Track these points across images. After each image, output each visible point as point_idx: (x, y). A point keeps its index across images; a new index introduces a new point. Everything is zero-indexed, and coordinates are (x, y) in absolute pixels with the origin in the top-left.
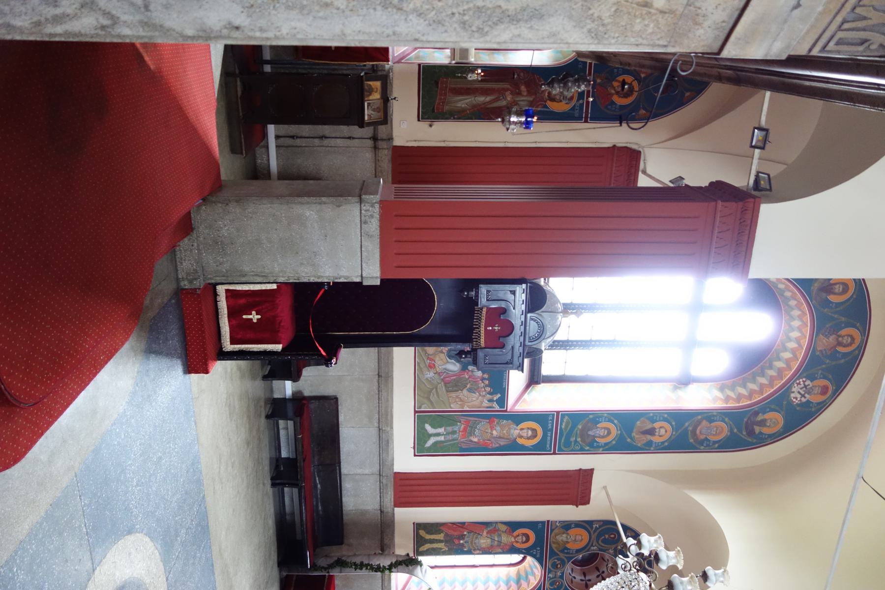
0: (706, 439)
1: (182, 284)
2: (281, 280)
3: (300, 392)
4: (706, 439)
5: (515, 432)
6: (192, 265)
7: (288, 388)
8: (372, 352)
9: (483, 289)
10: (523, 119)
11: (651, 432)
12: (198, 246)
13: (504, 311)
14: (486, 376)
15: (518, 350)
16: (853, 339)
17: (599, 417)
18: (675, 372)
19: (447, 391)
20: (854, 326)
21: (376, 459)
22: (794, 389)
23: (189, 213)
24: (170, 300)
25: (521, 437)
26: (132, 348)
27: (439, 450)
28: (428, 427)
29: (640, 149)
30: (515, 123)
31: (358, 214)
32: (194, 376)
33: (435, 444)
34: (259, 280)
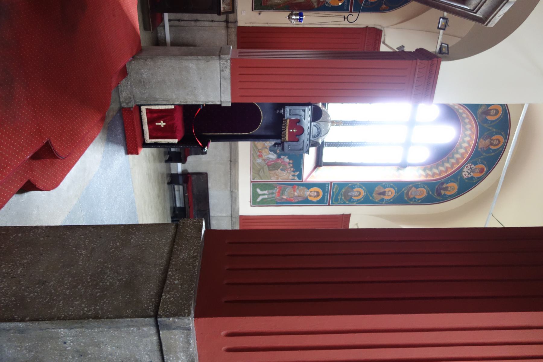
0: (414, 198)
1: (122, 105)
2: (177, 103)
3: (186, 170)
4: (414, 198)
5: (307, 193)
6: (128, 95)
7: (179, 167)
8: (227, 143)
9: (288, 109)
10: (298, 17)
11: (384, 193)
12: (131, 84)
13: (299, 121)
14: (291, 162)
15: (307, 142)
16: (499, 142)
17: (354, 185)
18: (399, 161)
19: (269, 170)
20: (501, 134)
21: (229, 208)
22: (464, 170)
23: (125, 65)
24: (117, 114)
25: (310, 196)
26: (100, 138)
27: (265, 203)
28: (258, 190)
29: (382, 29)
30: (294, 19)
31: (219, 66)
32: (130, 156)
33: (263, 199)
34: (165, 103)
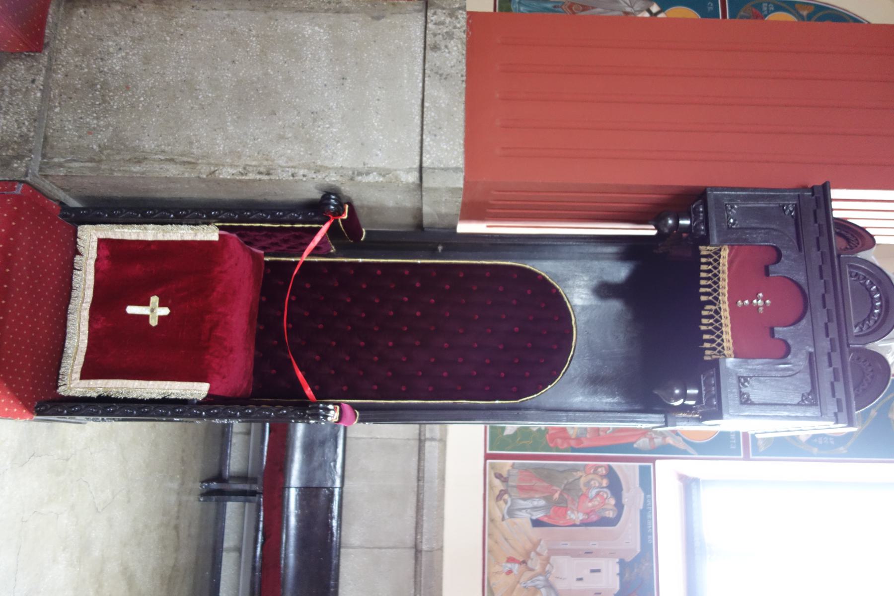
6: (20, 125)
31: (419, 33)
